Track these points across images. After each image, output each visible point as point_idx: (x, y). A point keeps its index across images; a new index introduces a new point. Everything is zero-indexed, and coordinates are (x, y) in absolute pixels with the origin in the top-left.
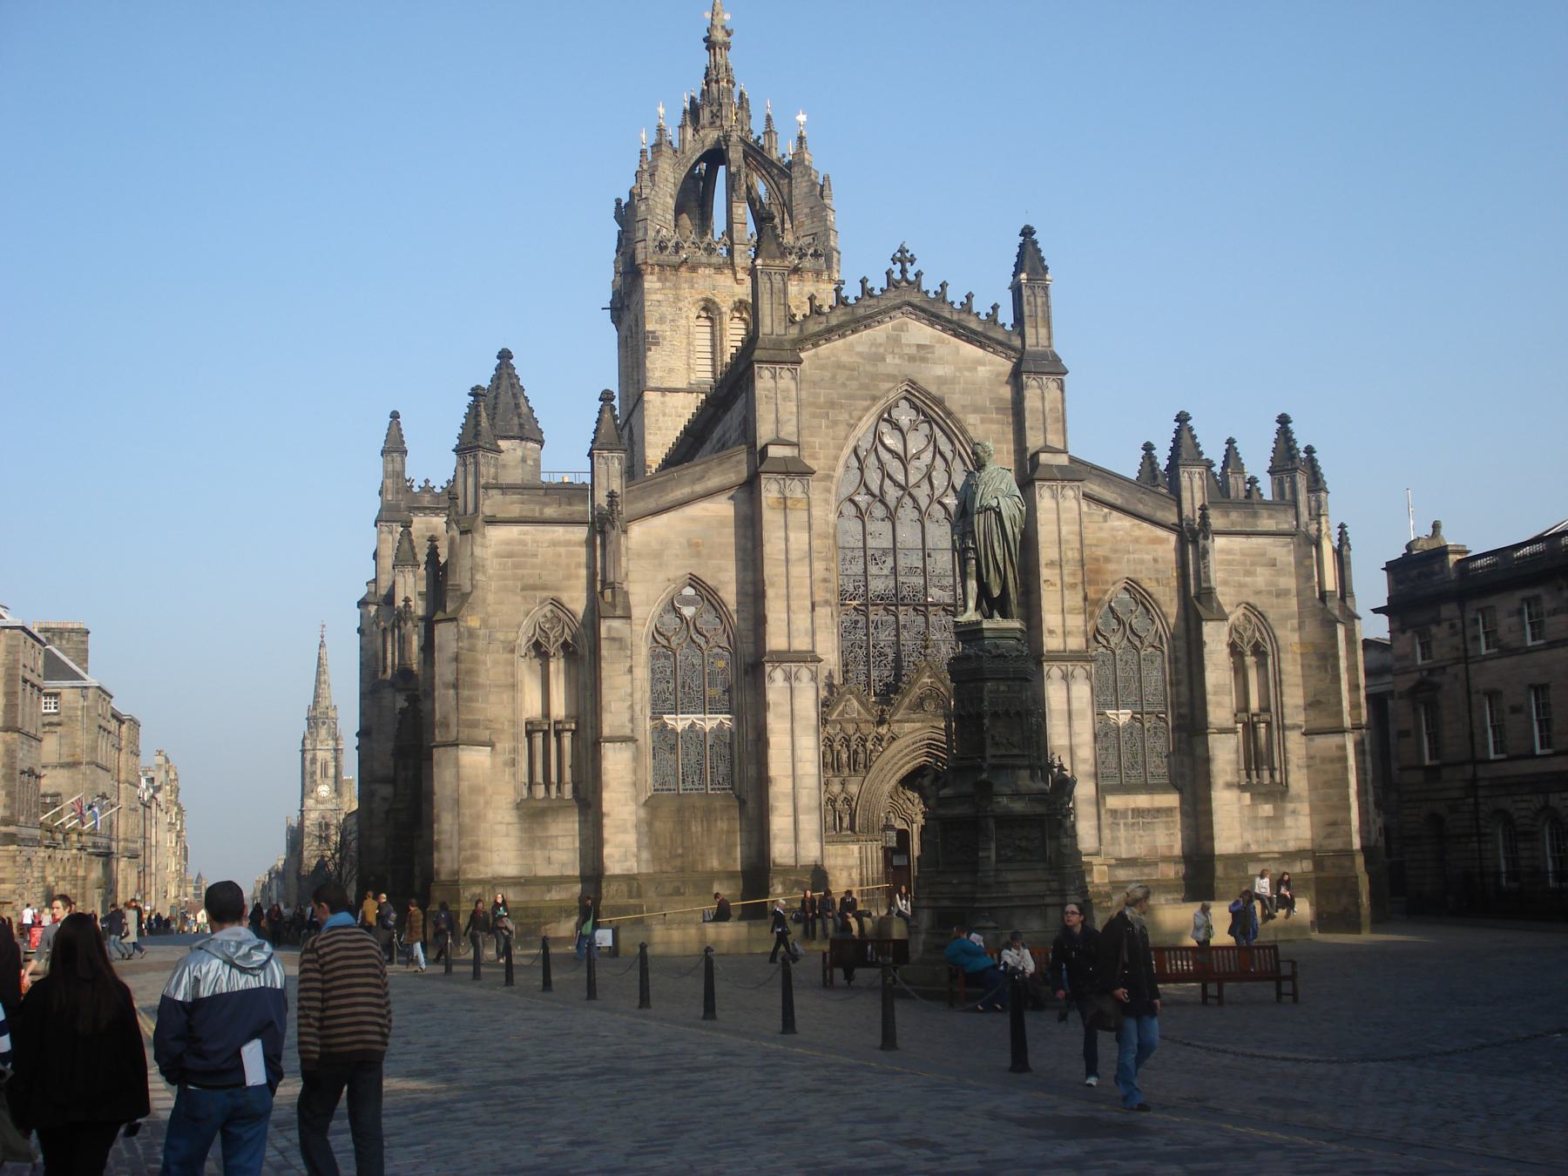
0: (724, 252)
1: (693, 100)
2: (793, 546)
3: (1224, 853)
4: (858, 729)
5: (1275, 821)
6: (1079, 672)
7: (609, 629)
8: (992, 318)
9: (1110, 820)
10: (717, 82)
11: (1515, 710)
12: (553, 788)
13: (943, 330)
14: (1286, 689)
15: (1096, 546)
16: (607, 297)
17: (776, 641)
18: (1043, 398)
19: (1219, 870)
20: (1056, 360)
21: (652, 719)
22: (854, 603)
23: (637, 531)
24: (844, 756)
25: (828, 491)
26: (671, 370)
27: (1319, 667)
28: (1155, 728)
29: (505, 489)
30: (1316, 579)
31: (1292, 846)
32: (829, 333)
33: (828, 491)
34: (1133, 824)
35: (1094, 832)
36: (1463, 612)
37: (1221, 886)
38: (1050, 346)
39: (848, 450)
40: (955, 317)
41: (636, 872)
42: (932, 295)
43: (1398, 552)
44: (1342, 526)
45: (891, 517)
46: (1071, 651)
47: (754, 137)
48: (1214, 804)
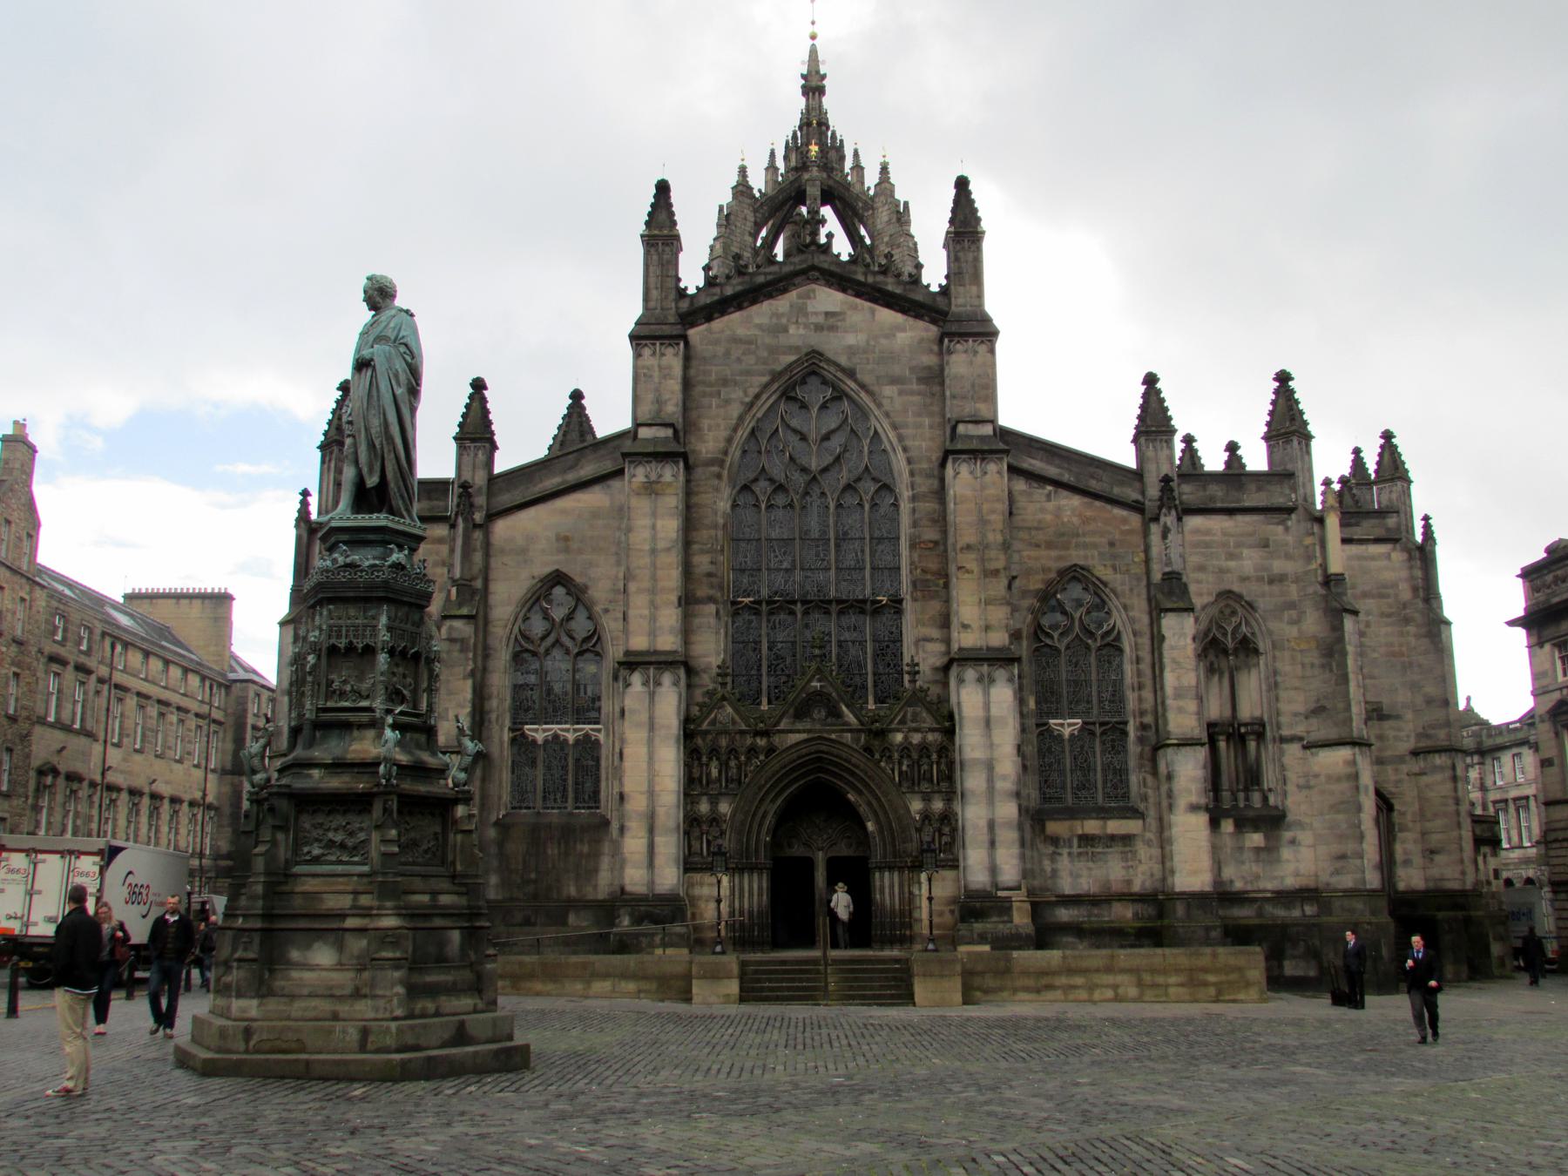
1: (787, 142)
2: (661, 535)
3: (1187, 890)
4: (733, 741)
5: (1268, 852)
6: (1001, 674)
7: (451, 628)
9: (1051, 849)
13: (858, 295)
14: (1283, 694)
15: (1037, 529)
18: (971, 363)
19: (1180, 909)
20: (986, 320)
21: (511, 730)
22: (747, 600)
23: (501, 527)
24: (715, 772)
25: (719, 476)
27: (1323, 666)
28: (1113, 740)
30: (1319, 561)
31: (1290, 882)
33: (719, 476)
34: (1080, 854)
35: (1015, 861)
37: (1181, 930)
38: (981, 305)
39: (743, 433)
40: (870, 279)
44: (1426, 518)
46: (988, 649)
48: (1175, 831)
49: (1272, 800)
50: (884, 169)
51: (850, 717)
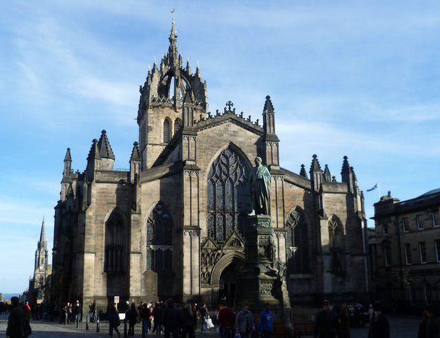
0: (173, 103)
7: (134, 217)
8: (257, 123)
10: (172, 51)
11: (415, 250)
12: (114, 268)
16: (136, 115)
17: (187, 223)
26: (155, 138)
29: (102, 172)
32: (205, 127)
36: (397, 218)
39: (210, 164)
41: (140, 295)
42: (238, 116)
43: (377, 200)
45: (223, 185)
47: (183, 68)
49: (343, 269)
50: (197, 69)
51: (243, 246)
